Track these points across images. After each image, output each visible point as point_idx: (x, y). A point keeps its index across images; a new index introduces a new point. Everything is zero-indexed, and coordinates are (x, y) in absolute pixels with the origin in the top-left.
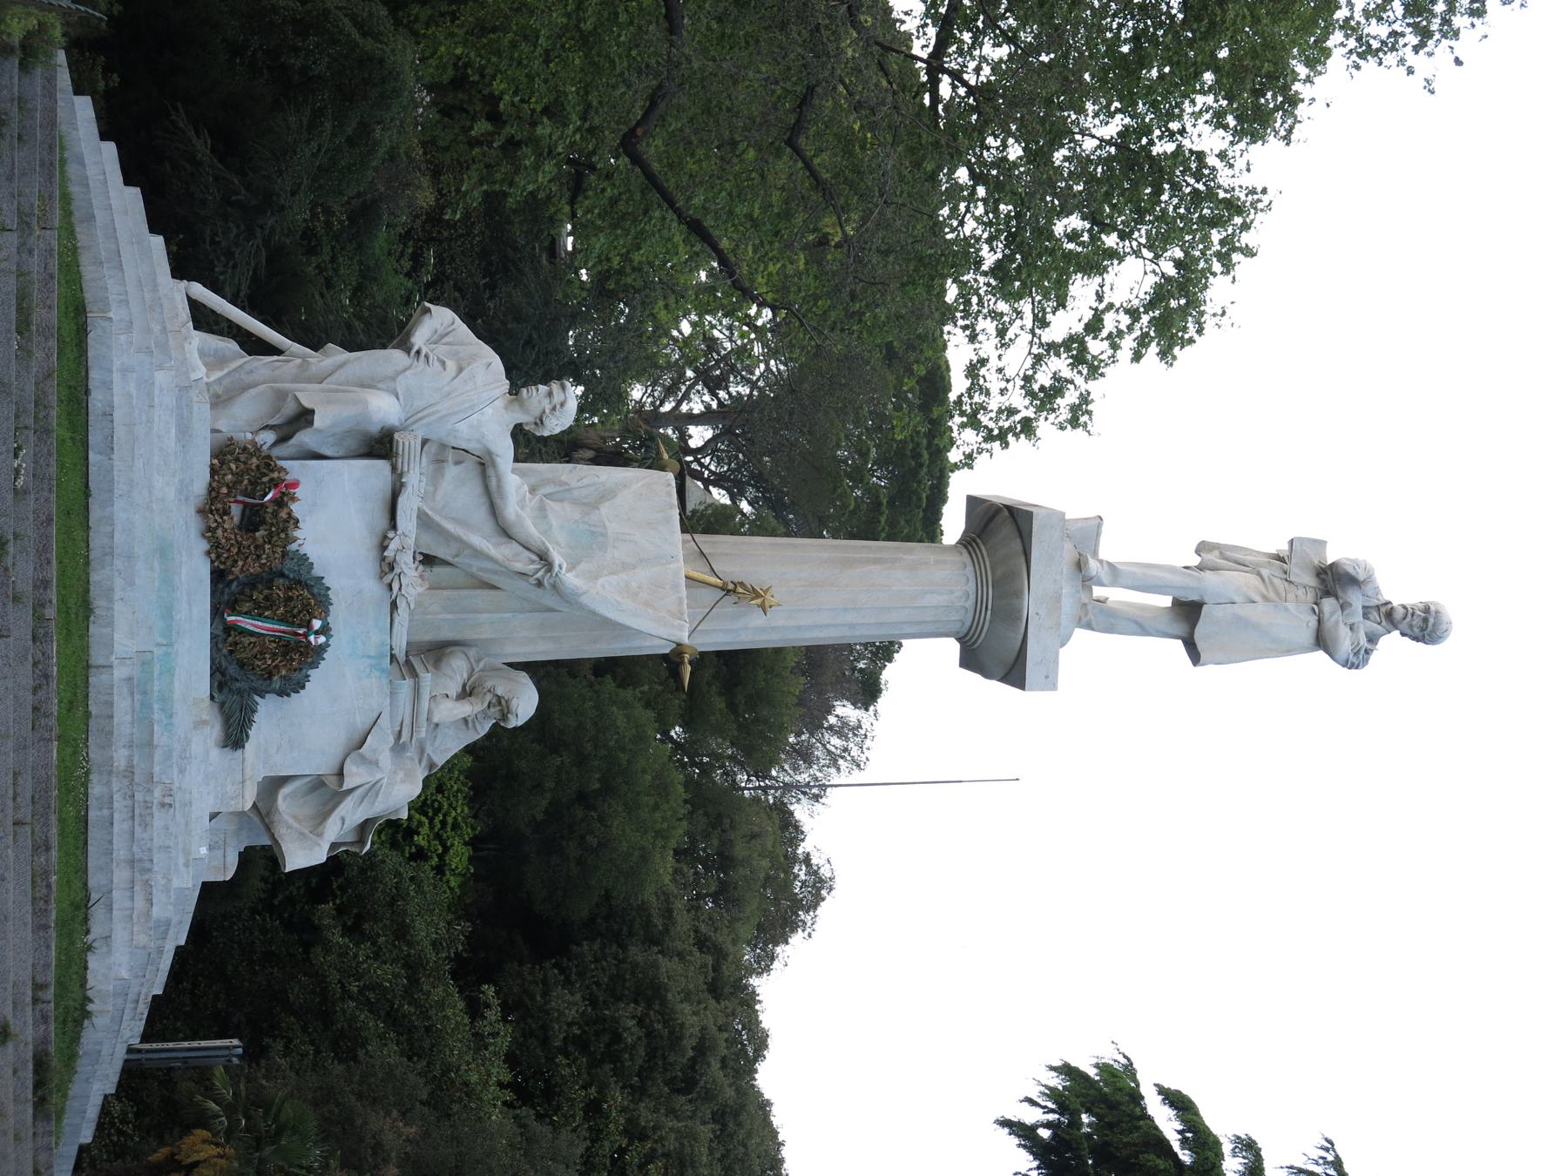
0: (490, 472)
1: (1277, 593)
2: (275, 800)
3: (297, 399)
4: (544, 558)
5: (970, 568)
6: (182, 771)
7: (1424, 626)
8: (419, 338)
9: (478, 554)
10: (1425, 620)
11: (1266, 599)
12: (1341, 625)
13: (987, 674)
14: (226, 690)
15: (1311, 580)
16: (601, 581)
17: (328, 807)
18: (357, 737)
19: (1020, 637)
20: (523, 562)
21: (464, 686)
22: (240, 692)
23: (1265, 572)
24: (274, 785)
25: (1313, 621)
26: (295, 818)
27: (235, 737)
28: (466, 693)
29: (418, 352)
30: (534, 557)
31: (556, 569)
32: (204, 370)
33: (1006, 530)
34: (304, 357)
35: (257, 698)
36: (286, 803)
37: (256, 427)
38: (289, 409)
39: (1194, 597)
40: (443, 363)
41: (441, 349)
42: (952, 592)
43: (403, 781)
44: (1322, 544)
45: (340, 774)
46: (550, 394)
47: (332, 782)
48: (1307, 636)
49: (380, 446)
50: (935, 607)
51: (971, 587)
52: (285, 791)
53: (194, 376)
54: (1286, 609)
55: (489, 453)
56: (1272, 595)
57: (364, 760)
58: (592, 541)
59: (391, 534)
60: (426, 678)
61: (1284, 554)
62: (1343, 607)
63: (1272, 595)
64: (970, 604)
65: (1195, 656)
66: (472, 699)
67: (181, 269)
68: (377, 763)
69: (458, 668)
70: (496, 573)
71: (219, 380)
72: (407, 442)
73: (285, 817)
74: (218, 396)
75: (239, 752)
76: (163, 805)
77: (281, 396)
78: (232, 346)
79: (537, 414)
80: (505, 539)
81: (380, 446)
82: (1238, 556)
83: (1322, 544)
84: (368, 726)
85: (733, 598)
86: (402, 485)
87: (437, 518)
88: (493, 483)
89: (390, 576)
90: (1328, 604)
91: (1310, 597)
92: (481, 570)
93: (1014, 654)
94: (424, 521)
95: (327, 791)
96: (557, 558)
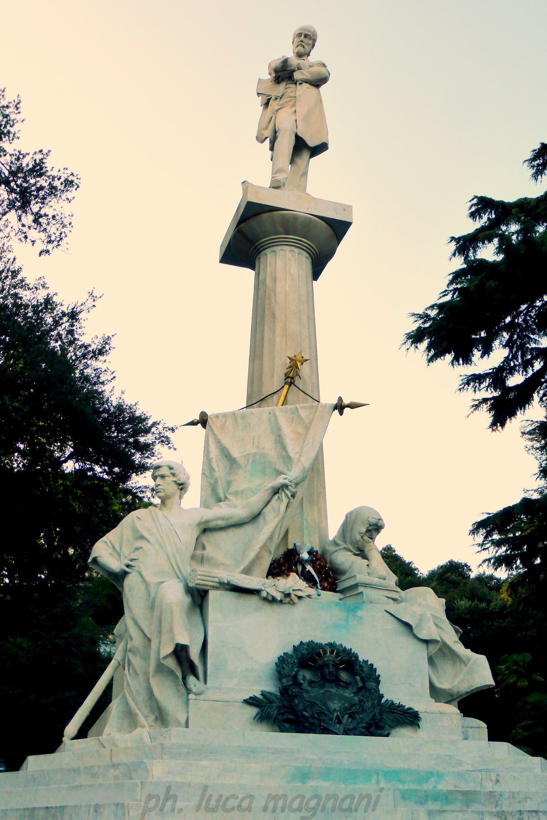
0: (212, 524)
1: (290, 101)
2: (443, 690)
3: (165, 657)
4: (276, 491)
5: (275, 248)
6: (460, 763)
7: (306, 39)
8: (115, 564)
9: (271, 538)
10: (306, 36)
11: (294, 105)
12: (309, 70)
13: (330, 254)
14: (381, 724)
15: (283, 85)
16: (292, 455)
17: (447, 652)
18: (401, 628)
20: (279, 504)
21: (355, 555)
22: (381, 714)
23: (277, 107)
24: (436, 693)
25: (305, 85)
26: (455, 676)
27: (410, 718)
28: (362, 553)
29: (128, 566)
30: (276, 496)
31: (286, 481)
32: (139, 730)
33: (253, 223)
34: (125, 650)
35: (383, 700)
36: (444, 684)
37: (183, 690)
38: (171, 663)
40: (137, 549)
41: (126, 551)
43: (425, 599)
44: (260, 81)
45: (426, 642)
46: (163, 477)
47: (433, 648)
48: (312, 89)
49: (198, 597)
52: (437, 684)
53: (147, 739)
54: (300, 96)
55: (199, 524)
56: (291, 103)
57: (419, 625)
58: (261, 464)
59: (264, 594)
60: (362, 578)
61: (265, 99)
62: (299, 69)
63: (291, 103)
64: (297, 250)
65: (322, 148)
66: (366, 550)
67: (51, 743)
68: (422, 615)
69: (343, 558)
70: (281, 527)
71: (146, 717)
72: (202, 575)
73: (456, 683)
74: (156, 718)
75: (421, 715)
76: (497, 781)
77: (161, 668)
78: (115, 706)
79: (175, 487)
80: (261, 519)
81: (198, 597)
82: (267, 120)
83: (260, 81)
84: (395, 621)
85: (297, 379)
86: (228, 584)
87: (246, 562)
88: (221, 523)
89: (293, 596)
90: (297, 76)
91: (293, 86)
92: (278, 539)
93: (329, 228)
94: (247, 571)
95: (437, 653)
96: (280, 480)
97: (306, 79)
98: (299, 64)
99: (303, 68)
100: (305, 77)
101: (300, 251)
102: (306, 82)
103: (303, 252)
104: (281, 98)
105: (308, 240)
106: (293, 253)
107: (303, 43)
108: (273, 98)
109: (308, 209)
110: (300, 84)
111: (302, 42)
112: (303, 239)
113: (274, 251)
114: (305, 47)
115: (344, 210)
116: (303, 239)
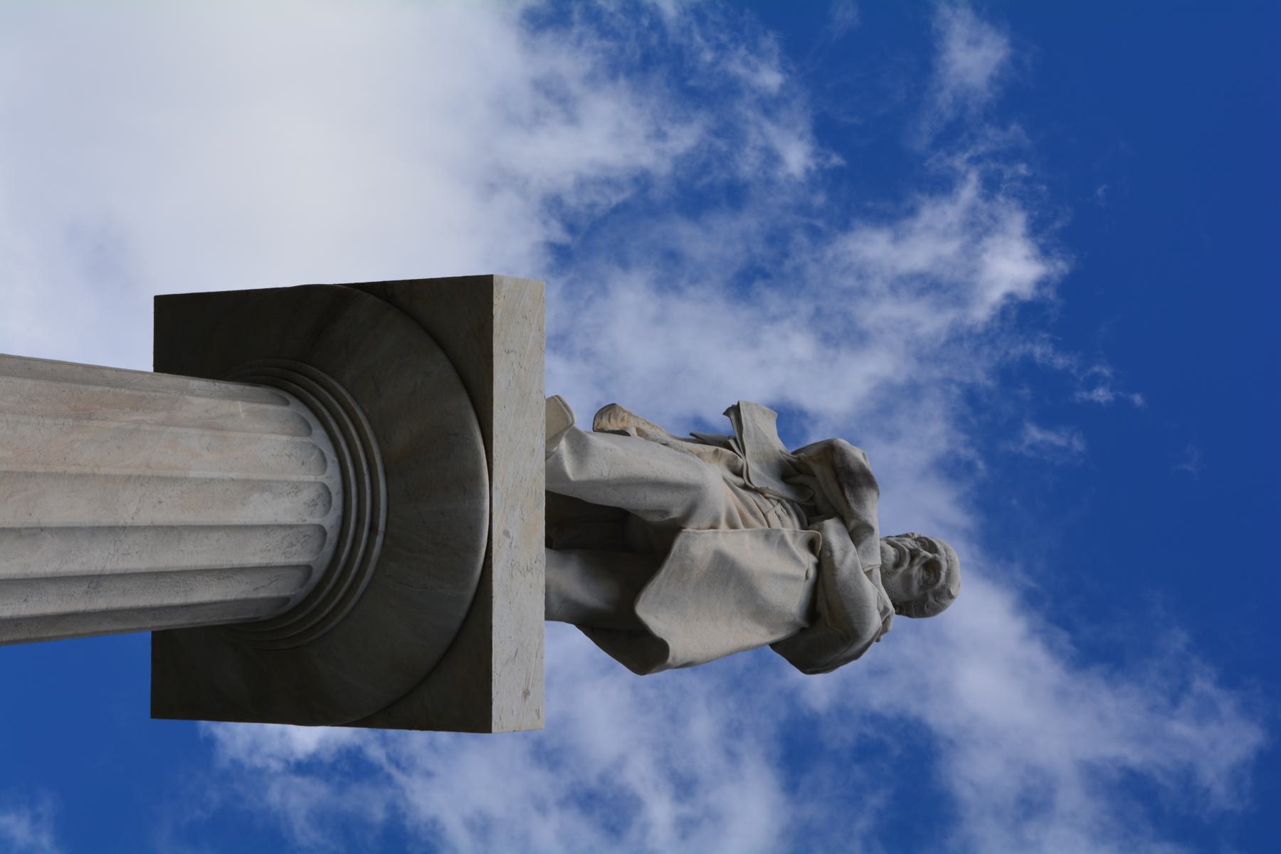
1: (754, 514)
5: (319, 432)
19: (470, 594)
39: (676, 513)
42: (297, 487)
50: (267, 528)
51: (332, 478)
54: (783, 543)
64: (330, 521)
97: (832, 563)
98: (870, 529)
99: (861, 547)
100: (838, 554)
101: (332, 536)
102: (819, 566)
103: (329, 549)
104: (745, 487)
105: (379, 561)
106: (320, 508)
107: (908, 559)
108: (741, 461)
109: (506, 533)
110: (812, 546)
111: (913, 558)
112: (379, 540)
113: (310, 428)
114: (901, 570)
115: (526, 694)
116: (379, 540)
